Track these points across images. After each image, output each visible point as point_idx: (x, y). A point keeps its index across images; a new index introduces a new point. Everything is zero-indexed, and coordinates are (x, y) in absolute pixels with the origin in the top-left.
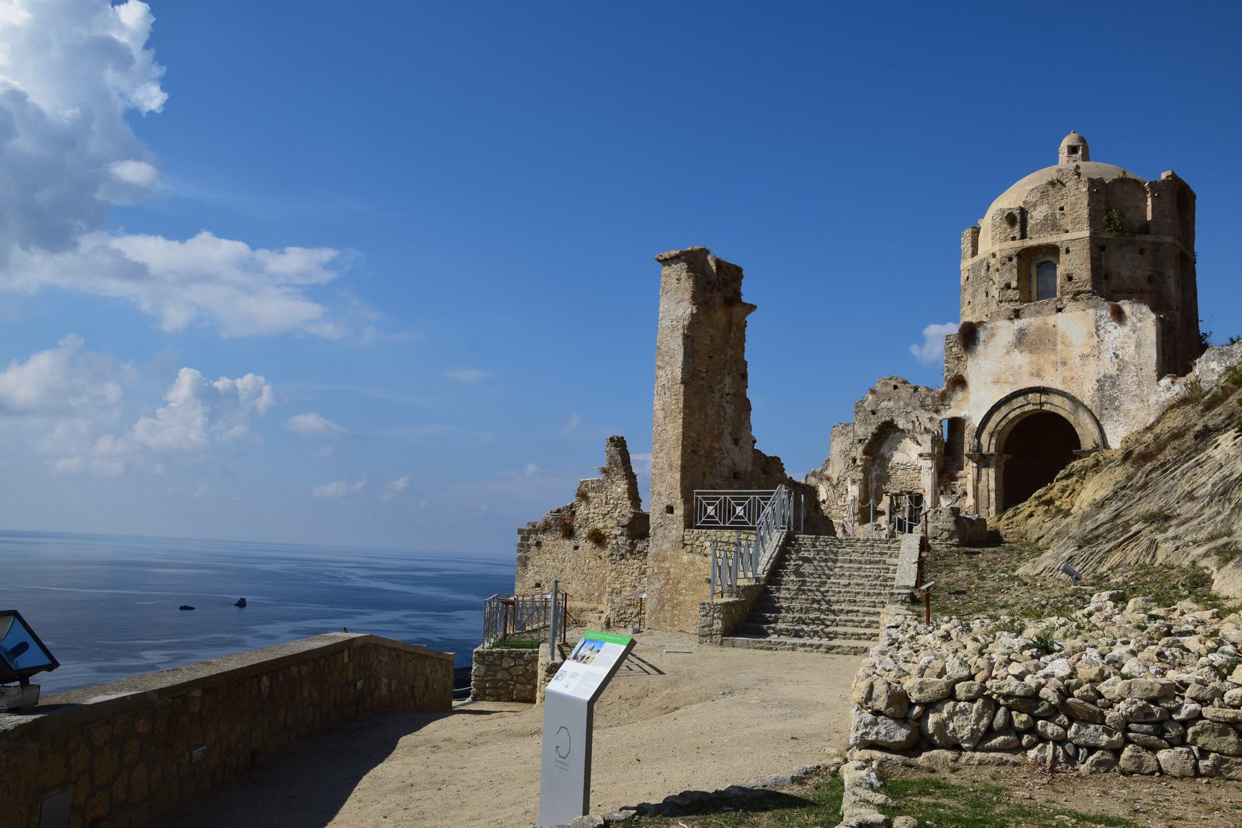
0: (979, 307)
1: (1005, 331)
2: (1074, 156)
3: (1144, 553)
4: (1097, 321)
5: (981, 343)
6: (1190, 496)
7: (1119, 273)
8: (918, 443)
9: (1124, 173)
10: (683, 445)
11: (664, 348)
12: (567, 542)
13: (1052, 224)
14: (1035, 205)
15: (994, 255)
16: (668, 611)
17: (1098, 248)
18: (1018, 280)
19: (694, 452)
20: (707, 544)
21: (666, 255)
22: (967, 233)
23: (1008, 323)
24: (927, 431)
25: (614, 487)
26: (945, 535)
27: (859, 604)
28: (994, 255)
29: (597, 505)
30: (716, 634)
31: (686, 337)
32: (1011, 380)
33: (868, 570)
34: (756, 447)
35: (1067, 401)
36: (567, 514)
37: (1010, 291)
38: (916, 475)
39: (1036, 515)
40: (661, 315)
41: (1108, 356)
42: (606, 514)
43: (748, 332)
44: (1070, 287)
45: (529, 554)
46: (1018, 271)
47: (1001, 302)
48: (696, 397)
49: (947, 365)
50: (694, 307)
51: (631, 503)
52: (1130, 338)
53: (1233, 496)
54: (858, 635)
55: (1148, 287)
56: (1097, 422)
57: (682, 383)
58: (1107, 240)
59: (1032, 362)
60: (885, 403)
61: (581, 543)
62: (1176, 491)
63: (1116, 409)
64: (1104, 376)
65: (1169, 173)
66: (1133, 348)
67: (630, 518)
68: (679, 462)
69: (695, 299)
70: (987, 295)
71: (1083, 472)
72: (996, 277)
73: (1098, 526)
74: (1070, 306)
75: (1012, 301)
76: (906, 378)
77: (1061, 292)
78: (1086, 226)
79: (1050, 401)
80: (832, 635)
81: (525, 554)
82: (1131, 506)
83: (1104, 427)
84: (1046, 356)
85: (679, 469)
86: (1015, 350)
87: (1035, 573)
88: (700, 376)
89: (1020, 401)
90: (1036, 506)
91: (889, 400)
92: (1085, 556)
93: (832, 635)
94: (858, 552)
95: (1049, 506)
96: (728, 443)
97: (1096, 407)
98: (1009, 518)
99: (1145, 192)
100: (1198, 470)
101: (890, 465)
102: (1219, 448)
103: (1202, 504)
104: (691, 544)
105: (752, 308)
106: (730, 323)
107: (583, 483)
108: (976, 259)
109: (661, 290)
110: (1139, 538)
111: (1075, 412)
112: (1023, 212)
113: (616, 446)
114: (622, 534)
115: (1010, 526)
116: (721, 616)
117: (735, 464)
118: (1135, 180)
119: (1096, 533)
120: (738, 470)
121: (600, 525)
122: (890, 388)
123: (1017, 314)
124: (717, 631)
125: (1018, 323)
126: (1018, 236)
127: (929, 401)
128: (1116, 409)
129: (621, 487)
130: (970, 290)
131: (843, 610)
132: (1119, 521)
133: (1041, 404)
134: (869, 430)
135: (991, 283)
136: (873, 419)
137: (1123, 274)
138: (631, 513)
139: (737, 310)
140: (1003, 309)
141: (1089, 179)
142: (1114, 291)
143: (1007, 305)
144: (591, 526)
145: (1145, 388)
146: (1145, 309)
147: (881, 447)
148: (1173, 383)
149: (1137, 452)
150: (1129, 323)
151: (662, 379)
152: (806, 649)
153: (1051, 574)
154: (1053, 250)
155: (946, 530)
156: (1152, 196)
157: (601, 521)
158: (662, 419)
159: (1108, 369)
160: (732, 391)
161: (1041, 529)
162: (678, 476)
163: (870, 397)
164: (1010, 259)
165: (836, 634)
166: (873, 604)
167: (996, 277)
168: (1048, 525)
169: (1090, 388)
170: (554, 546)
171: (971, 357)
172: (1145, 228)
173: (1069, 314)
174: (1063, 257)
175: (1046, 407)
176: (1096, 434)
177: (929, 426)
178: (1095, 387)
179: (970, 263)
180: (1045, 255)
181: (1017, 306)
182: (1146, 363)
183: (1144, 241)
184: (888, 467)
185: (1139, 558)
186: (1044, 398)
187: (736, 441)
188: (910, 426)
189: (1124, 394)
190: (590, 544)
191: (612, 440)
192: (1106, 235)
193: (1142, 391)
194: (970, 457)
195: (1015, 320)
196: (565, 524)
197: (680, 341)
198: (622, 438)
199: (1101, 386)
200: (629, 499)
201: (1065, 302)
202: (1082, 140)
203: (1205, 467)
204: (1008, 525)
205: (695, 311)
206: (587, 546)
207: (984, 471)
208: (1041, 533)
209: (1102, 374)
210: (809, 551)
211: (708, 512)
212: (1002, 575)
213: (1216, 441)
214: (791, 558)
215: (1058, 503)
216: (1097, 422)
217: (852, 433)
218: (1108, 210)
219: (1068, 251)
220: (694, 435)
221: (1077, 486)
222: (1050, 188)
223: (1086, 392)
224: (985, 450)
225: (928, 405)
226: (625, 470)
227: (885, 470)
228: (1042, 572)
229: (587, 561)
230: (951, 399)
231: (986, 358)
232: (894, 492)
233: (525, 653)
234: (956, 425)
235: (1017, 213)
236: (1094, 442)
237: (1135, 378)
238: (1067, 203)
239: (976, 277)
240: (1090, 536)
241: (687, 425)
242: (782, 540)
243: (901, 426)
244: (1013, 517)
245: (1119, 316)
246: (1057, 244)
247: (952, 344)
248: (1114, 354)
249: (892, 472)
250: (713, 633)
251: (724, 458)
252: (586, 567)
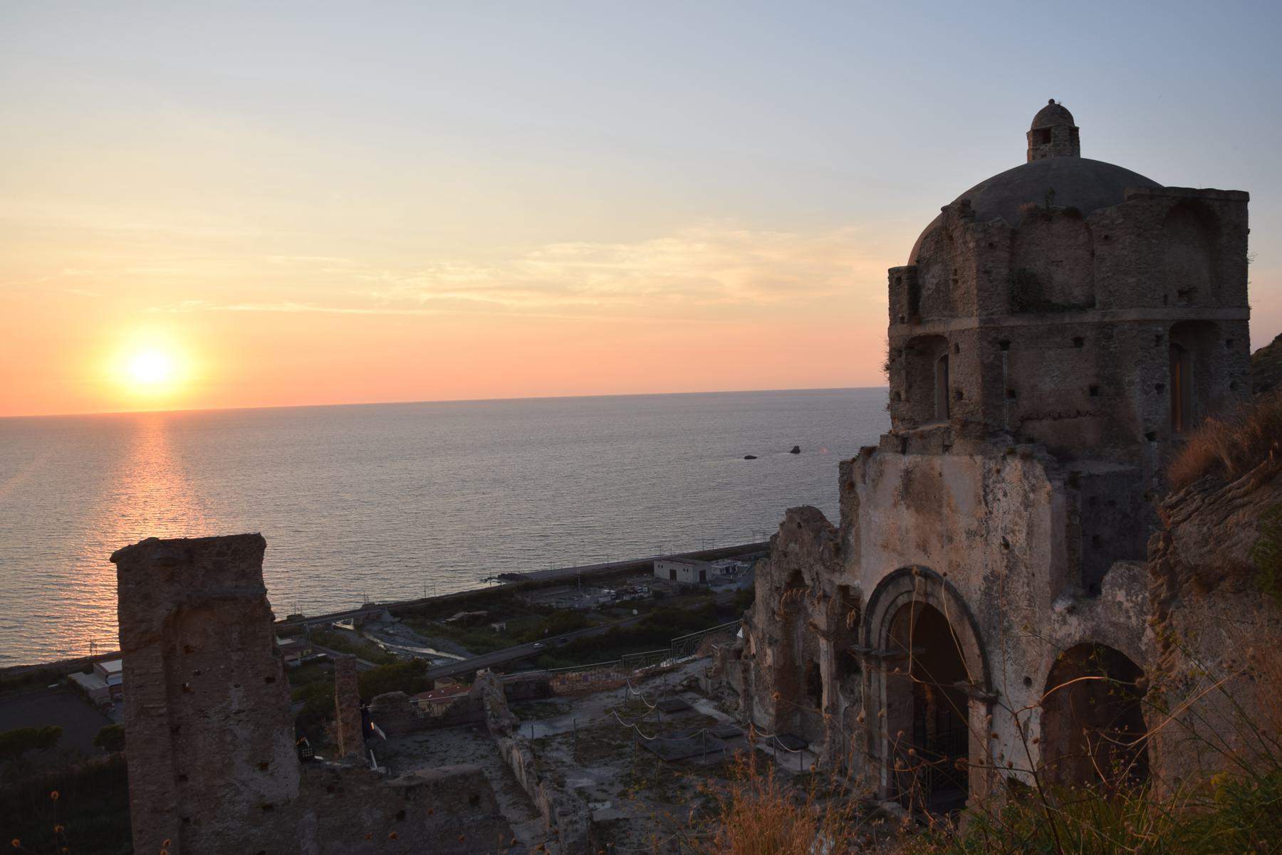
2: (1042, 147)
4: (984, 478)
41: (996, 541)
52: (1021, 517)
66: (1024, 534)
84: (932, 521)
86: (902, 502)
159: (996, 562)
169: (977, 589)
173: (956, 458)
189: (1014, 610)
193: (1034, 613)
201: (953, 437)
237: (1026, 589)
246: (945, 336)
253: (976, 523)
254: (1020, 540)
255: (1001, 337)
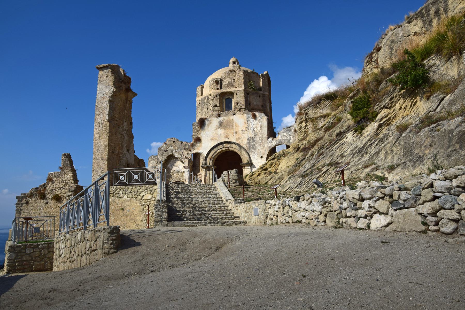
0: (204, 113)
1: (215, 121)
3: (334, 177)
5: (206, 126)
6: (342, 156)
7: (253, 103)
8: (183, 163)
9: (254, 70)
10: (108, 149)
11: (99, 106)
12: (42, 201)
13: (231, 85)
14: (225, 78)
15: (210, 95)
16: (102, 224)
17: (247, 94)
18: (219, 104)
19: (113, 152)
20: (121, 192)
21: (102, 66)
22: (199, 88)
23: (216, 118)
24: (186, 158)
25: (66, 175)
26: (233, 181)
27: (213, 208)
28: (210, 95)
29: (57, 184)
30: (164, 221)
31: (110, 101)
32: (218, 139)
33: (208, 195)
34: (135, 154)
35: (237, 146)
36: (42, 189)
37: (216, 107)
38: (182, 175)
39: (261, 175)
40: (98, 91)
41: (251, 130)
42: (62, 187)
43: (133, 105)
44: (238, 107)
45: (22, 208)
46: (219, 101)
47: (213, 111)
48: (114, 128)
49: (194, 133)
50: (114, 88)
51: (74, 182)
52: (258, 124)
53: (368, 151)
54: (228, 218)
55: (261, 109)
56: (248, 153)
57: (108, 121)
58: (250, 91)
59: (225, 133)
60: (170, 148)
61: (49, 201)
62: (335, 155)
63: (254, 149)
64: (250, 138)
65: (267, 72)
67: (75, 188)
68: (107, 156)
69: (114, 85)
70: (208, 109)
71: (279, 157)
72: (211, 102)
73: (307, 170)
74: (238, 113)
75: (217, 111)
76: (178, 139)
77: (235, 108)
78: (243, 86)
79: (232, 146)
80: (216, 219)
81: (20, 208)
82: (318, 161)
83: (250, 155)
85: (107, 159)
87: (284, 190)
88: (116, 119)
89: (221, 146)
90: (261, 171)
91: (172, 147)
92: (307, 181)
93: (216, 219)
94: (199, 189)
95: (266, 171)
96: (125, 151)
97: (247, 148)
98: (250, 177)
99: (260, 77)
100: (343, 146)
101: (171, 171)
102: (348, 138)
103: (350, 157)
104: (113, 193)
105: (135, 95)
106: (127, 100)
107: (50, 174)
108: (203, 97)
109: (98, 81)
110: (328, 172)
111: (240, 150)
112: (221, 80)
113: (67, 157)
114: (71, 195)
115: (251, 180)
116: (167, 211)
117: (128, 160)
118: (257, 73)
119: (306, 173)
120: (129, 163)
121: (59, 192)
122: (172, 142)
123: (219, 116)
124: (165, 219)
125: (220, 119)
126: (219, 88)
127: (187, 147)
128: (254, 149)
129: (69, 175)
130: (200, 108)
131: (210, 210)
132: (314, 168)
133: (228, 147)
134: (164, 158)
135: (209, 104)
136: (165, 154)
137: (254, 103)
138: (75, 185)
139: (130, 94)
140: (214, 114)
141: (244, 70)
142: (252, 109)
143: (215, 112)
144: (54, 193)
145: (264, 142)
146: (263, 115)
147: (168, 165)
148: (273, 140)
149: (302, 148)
150: (258, 119)
151: (98, 120)
152: (211, 224)
153: (292, 190)
154: (232, 94)
155: (233, 179)
156: (262, 79)
157: (59, 190)
158: (98, 138)
160: (127, 129)
161: (266, 179)
162: (106, 162)
163: (164, 146)
164: (217, 96)
165: (217, 218)
166: (220, 207)
167: (211, 102)
168: (269, 177)
170: (35, 203)
171: (203, 130)
172: (260, 89)
173: (238, 116)
174: (235, 96)
175: (230, 149)
176: (248, 158)
177: (187, 156)
178: (247, 141)
179: (201, 98)
180: (228, 95)
181: (219, 113)
182: (264, 133)
183: (260, 93)
184: (170, 172)
185: (332, 179)
186: (229, 145)
187: (128, 151)
188: (180, 156)
190: (54, 201)
191: (65, 154)
192: (249, 90)
194: (203, 167)
195: (219, 118)
196: (42, 193)
197: (108, 103)
198: (69, 154)
199: (249, 141)
200: (73, 180)
201: (236, 112)
202: (237, 60)
203: (345, 145)
204: (250, 179)
205: (115, 90)
206: (52, 202)
207: (208, 172)
208: (267, 181)
209: (249, 136)
210: (178, 189)
211: (121, 178)
212: (270, 193)
213: (346, 136)
214: (171, 192)
215: (269, 170)
216: (248, 153)
217: (157, 159)
218: (249, 81)
219: (237, 94)
220: (113, 145)
221: (278, 163)
222: (230, 72)
223: (244, 143)
224: (208, 165)
225: (187, 148)
226: (71, 168)
227: (169, 173)
228: (288, 190)
229: (52, 209)
230: (195, 146)
231: (208, 131)
232: (173, 181)
233: (39, 245)
234: (196, 156)
235: (219, 80)
236: (247, 160)
237: (260, 138)
238: (236, 78)
239: (203, 103)
240: (303, 175)
241: (110, 140)
242: (165, 185)
243: (176, 156)
244: (252, 176)
245: (255, 117)
247: (195, 126)
248: (253, 130)
249: (172, 174)
250: (163, 220)
251: (124, 157)
252: (51, 212)
253: (245, 128)
254: (258, 129)
255: (248, 92)
